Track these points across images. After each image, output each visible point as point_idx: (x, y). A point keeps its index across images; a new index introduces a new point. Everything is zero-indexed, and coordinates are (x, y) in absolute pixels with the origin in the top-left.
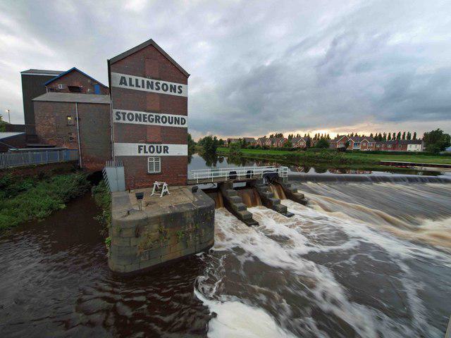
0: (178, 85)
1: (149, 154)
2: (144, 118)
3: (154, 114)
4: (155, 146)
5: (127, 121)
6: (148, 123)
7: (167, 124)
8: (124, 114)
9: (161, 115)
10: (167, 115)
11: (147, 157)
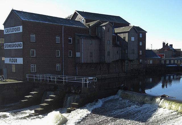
0: (18, 27)
2: (11, 46)
3: (13, 43)
4: (13, 58)
5: (7, 48)
6: (12, 48)
7: (17, 48)
8: (6, 45)
9: (15, 43)
10: (16, 43)
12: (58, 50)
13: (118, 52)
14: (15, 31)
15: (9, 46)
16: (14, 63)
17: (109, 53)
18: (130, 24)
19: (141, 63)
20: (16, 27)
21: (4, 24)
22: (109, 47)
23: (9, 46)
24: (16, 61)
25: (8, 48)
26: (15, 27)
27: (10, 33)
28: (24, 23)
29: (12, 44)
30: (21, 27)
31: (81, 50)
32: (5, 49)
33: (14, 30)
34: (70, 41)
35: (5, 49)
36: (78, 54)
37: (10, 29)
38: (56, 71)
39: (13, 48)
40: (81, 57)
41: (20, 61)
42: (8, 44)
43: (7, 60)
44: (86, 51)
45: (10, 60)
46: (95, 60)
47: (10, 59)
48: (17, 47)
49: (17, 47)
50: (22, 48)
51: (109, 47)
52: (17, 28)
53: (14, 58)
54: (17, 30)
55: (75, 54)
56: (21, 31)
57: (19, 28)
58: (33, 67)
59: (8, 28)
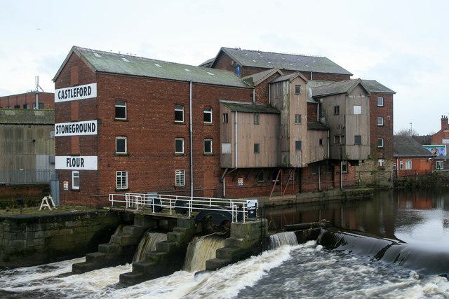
0: (87, 86)
1: (72, 168)
4: (76, 158)
5: (61, 134)
6: (72, 134)
7: (83, 133)
8: (60, 126)
9: (79, 123)
10: (83, 123)
11: (71, 171)
12: (181, 139)
13: (321, 141)
14: (81, 95)
15: (67, 129)
16: (76, 168)
17: (298, 144)
18: (352, 75)
19: (382, 169)
20: (83, 86)
21: (55, 80)
22: (298, 131)
23: (67, 129)
24: (82, 163)
25: (63, 133)
26: (80, 87)
27: (68, 99)
28: (101, 77)
29: (72, 124)
30: (94, 86)
31: (233, 140)
32: (56, 135)
33: (76, 93)
34: (207, 117)
35: (59, 135)
36: (226, 148)
37: (69, 90)
38: (175, 187)
39: (75, 134)
40: (233, 153)
41: (91, 163)
42: (65, 124)
43: (61, 163)
44: (244, 142)
45: (68, 162)
46: (265, 160)
47: (68, 159)
48: (85, 131)
49: (85, 131)
50: (95, 133)
51: (298, 131)
52: (85, 88)
53: (78, 157)
54: (85, 92)
55: (218, 148)
56: (94, 94)
57: (89, 87)
58: (121, 176)
59: (64, 89)
